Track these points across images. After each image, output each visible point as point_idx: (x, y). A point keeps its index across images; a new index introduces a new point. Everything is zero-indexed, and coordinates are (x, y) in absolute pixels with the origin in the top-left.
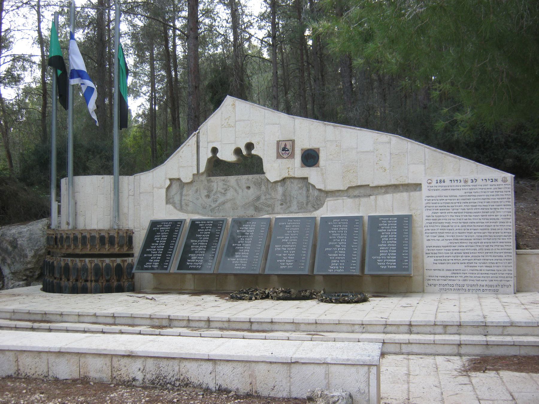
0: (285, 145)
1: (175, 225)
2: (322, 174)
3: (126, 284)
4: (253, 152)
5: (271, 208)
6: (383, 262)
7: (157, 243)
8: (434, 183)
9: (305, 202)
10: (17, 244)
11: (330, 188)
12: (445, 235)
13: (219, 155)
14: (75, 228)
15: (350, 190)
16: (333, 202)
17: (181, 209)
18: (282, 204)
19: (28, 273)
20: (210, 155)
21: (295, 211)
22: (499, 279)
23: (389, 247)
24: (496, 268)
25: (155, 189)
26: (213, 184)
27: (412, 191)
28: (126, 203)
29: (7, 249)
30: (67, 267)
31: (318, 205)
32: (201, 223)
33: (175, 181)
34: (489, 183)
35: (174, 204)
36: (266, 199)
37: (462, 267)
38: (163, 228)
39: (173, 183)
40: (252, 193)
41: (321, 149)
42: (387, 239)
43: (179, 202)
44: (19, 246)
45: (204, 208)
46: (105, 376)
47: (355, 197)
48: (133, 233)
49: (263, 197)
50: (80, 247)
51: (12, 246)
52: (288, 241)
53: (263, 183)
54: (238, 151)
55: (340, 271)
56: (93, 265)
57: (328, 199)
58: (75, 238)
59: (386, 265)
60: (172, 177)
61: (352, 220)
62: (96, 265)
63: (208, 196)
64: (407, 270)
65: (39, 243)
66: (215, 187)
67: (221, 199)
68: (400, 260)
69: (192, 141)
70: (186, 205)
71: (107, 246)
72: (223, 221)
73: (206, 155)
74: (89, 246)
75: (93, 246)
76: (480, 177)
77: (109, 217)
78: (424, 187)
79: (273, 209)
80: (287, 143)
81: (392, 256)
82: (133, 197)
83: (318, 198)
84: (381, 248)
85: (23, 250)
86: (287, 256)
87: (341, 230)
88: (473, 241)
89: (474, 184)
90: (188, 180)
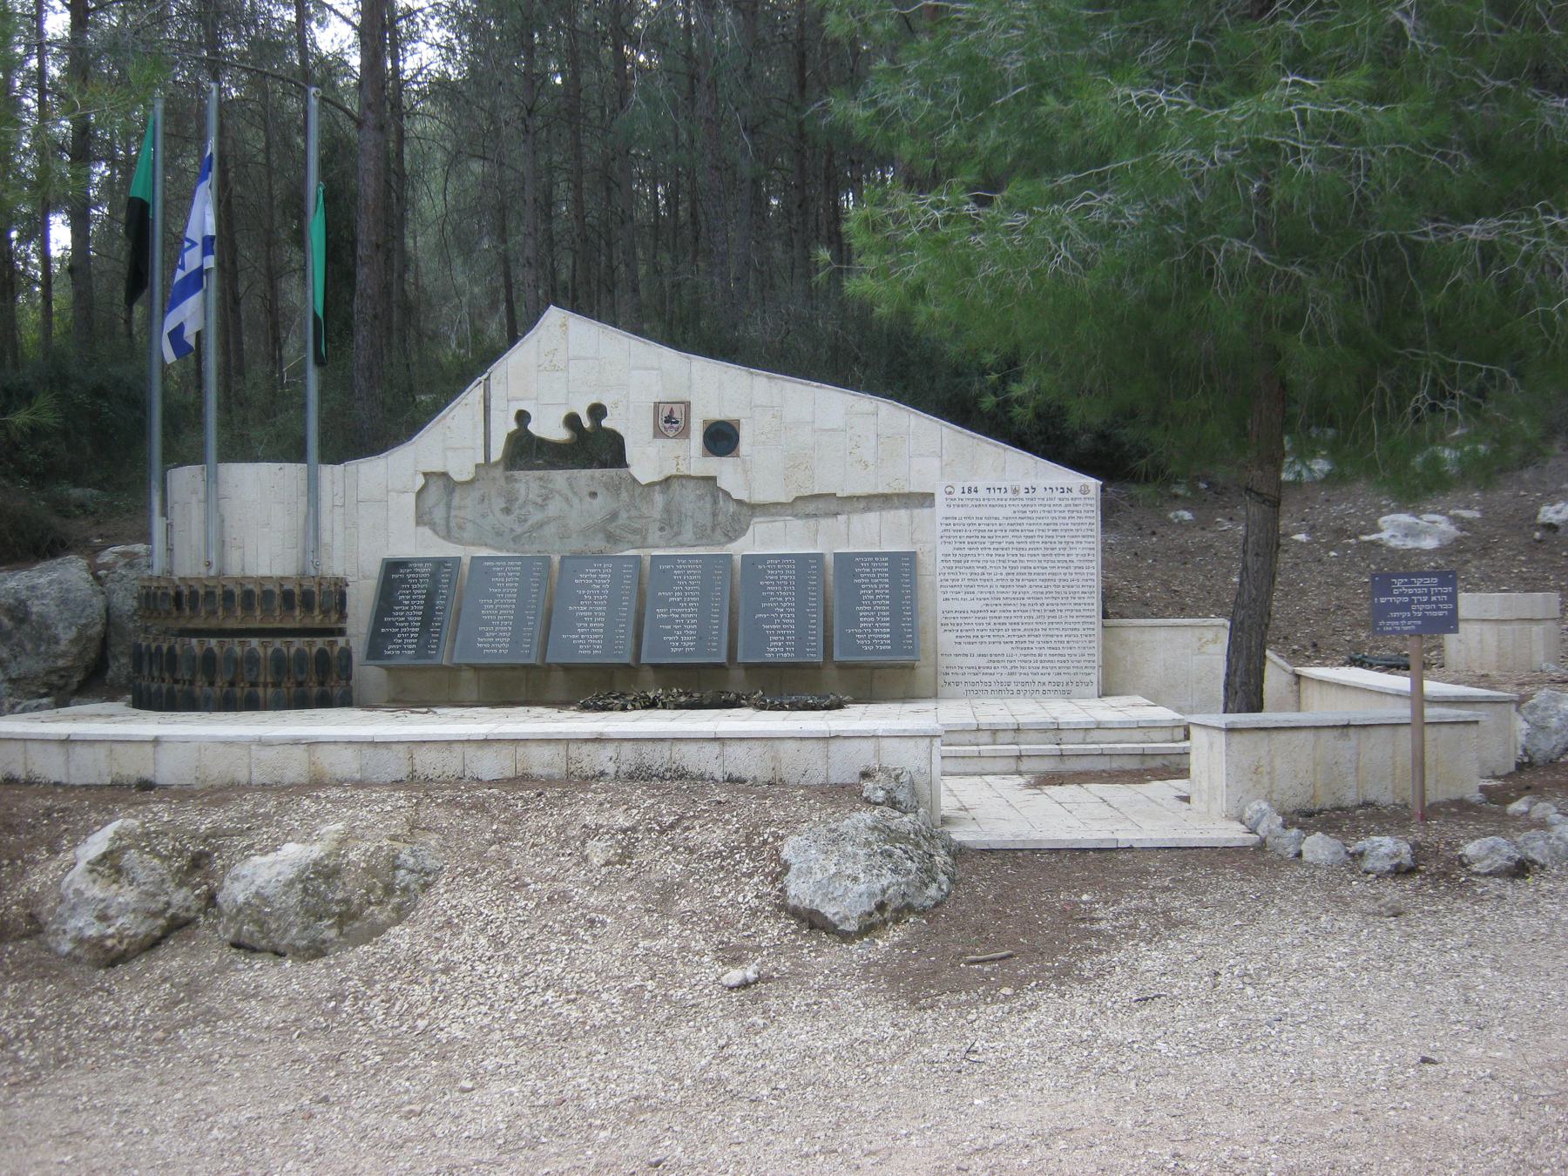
2: (745, 471)
4: (605, 423)
8: (957, 494)
9: (709, 525)
10: (27, 613)
11: (760, 497)
12: (976, 589)
13: (532, 427)
14: (221, 573)
17: (448, 536)
18: (662, 529)
19: (54, 678)
20: (513, 426)
22: (1072, 671)
24: (1067, 652)
26: (517, 486)
30: (209, 657)
31: (735, 531)
34: (1057, 494)
37: (1007, 649)
40: (600, 506)
43: (443, 522)
44: (34, 617)
45: (499, 534)
46: (558, 770)
47: (808, 516)
50: (239, 613)
51: (12, 618)
54: (572, 421)
55: (787, 657)
56: (270, 651)
58: (228, 596)
60: (429, 470)
61: (802, 560)
62: (277, 651)
63: (507, 511)
64: (908, 652)
65: (89, 611)
67: (536, 517)
68: (897, 635)
69: (473, 394)
70: (460, 528)
71: (297, 612)
73: (503, 426)
74: (258, 613)
75: (268, 612)
76: (1041, 483)
78: (940, 499)
79: (645, 538)
83: (735, 518)
85: (48, 627)
86: (682, 629)
88: (1026, 601)
89: (1030, 495)
90: (466, 477)
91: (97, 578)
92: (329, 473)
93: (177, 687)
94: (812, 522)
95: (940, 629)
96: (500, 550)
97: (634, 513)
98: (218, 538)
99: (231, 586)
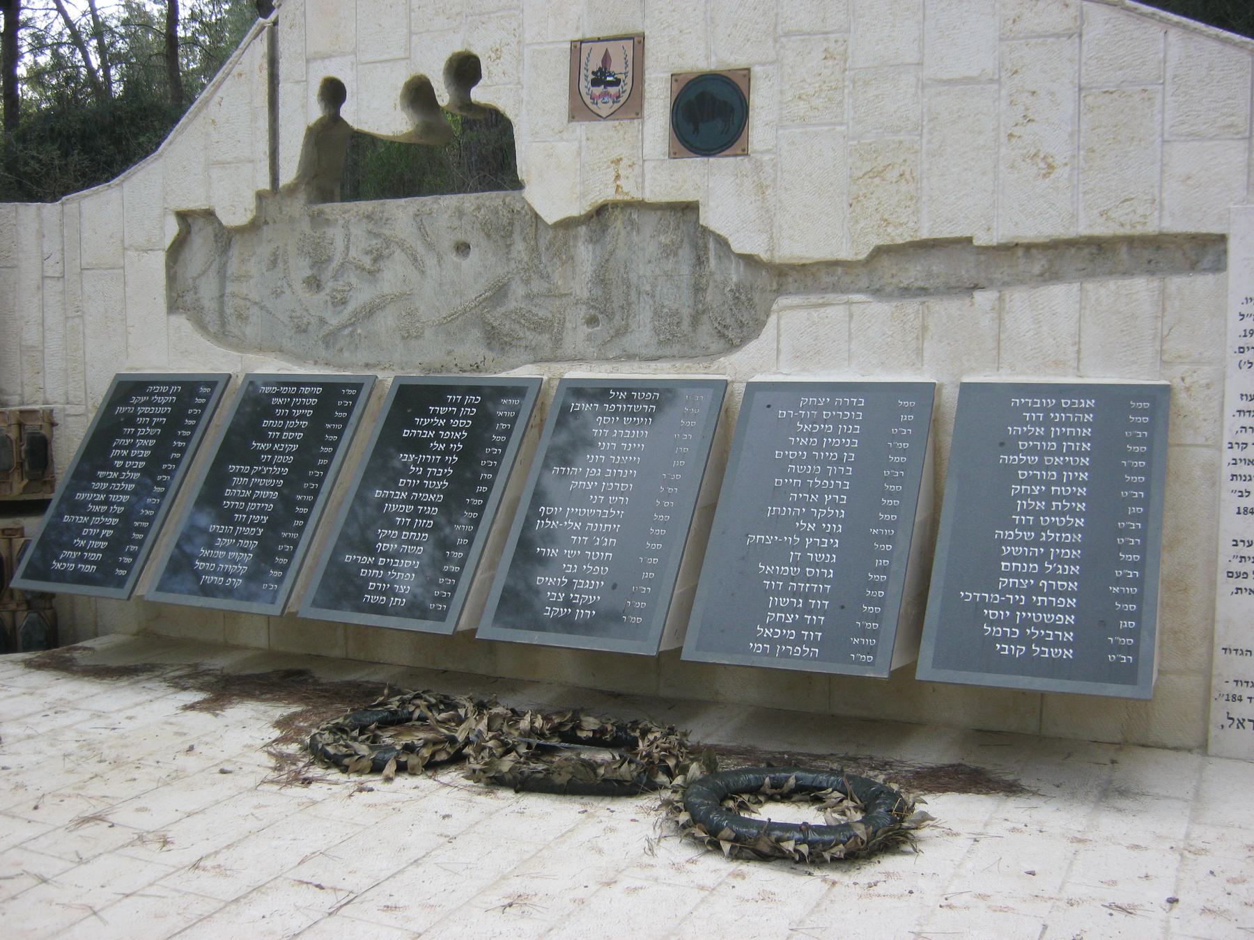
0: (606, 59)
1: (190, 394)
2: (761, 189)
4: (478, 94)
5: (548, 337)
6: (1010, 622)
7: (114, 469)
9: (686, 312)
15: (885, 261)
16: (803, 314)
18: (592, 321)
20: (316, 112)
21: (644, 352)
23: (1047, 545)
25: (131, 253)
26: (330, 232)
27: (1178, 271)
31: (739, 328)
32: (278, 395)
36: (529, 297)
38: (146, 409)
39: (195, 229)
40: (474, 272)
41: (757, 71)
42: (1041, 505)
45: (302, 330)
47: (906, 292)
49: (518, 290)
52: (595, 491)
53: (517, 228)
54: (418, 94)
55: (803, 656)
57: (783, 301)
59: (1024, 640)
60: (185, 206)
63: (314, 283)
64: (1128, 674)
66: (340, 243)
67: (362, 296)
72: (358, 387)
73: (302, 111)
79: (557, 341)
80: (615, 49)
81: (1057, 594)
82: (59, 286)
84: (1006, 550)
87: (830, 448)
94: (912, 307)
95: (1226, 587)
96: (300, 358)
97: (537, 286)
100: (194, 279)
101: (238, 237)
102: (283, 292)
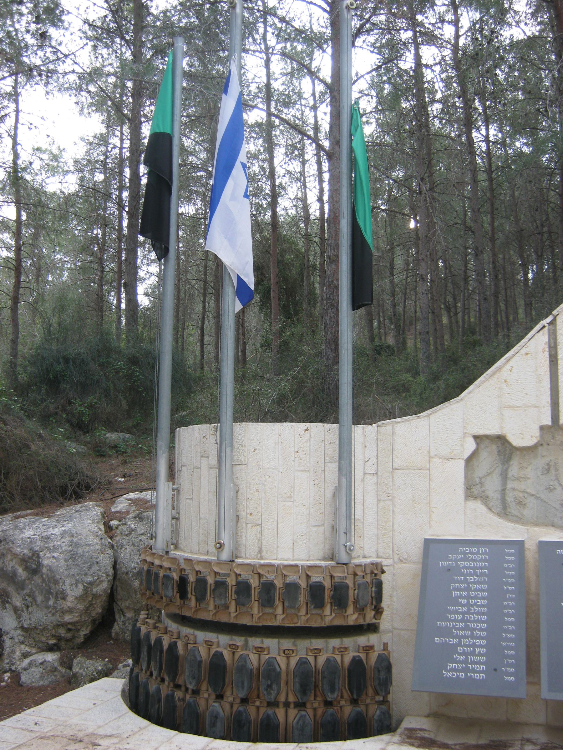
3: (374, 712)
10: (39, 565)
17: (504, 512)
19: (62, 632)
25: (436, 460)
28: (364, 491)
29: (15, 574)
33: (487, 442)
35: (485, 499)
43: (498, 496)
44: (44, 570)
48: (383, 572)
51: (26, 568)
56: (293, 662)
58: (243, 588)
60: (481, 432)
65: (95, 568)
69: (535, 342)
70: (520, 503)
77: (321, 529)
82: (374, 479)
91: (109, 529)
92: (364, 435)
93: (178, 694)
98: (229, 508)
99: (246, 576)
100: (480, 478)
101: (518, 453)
102: (555, 489)
